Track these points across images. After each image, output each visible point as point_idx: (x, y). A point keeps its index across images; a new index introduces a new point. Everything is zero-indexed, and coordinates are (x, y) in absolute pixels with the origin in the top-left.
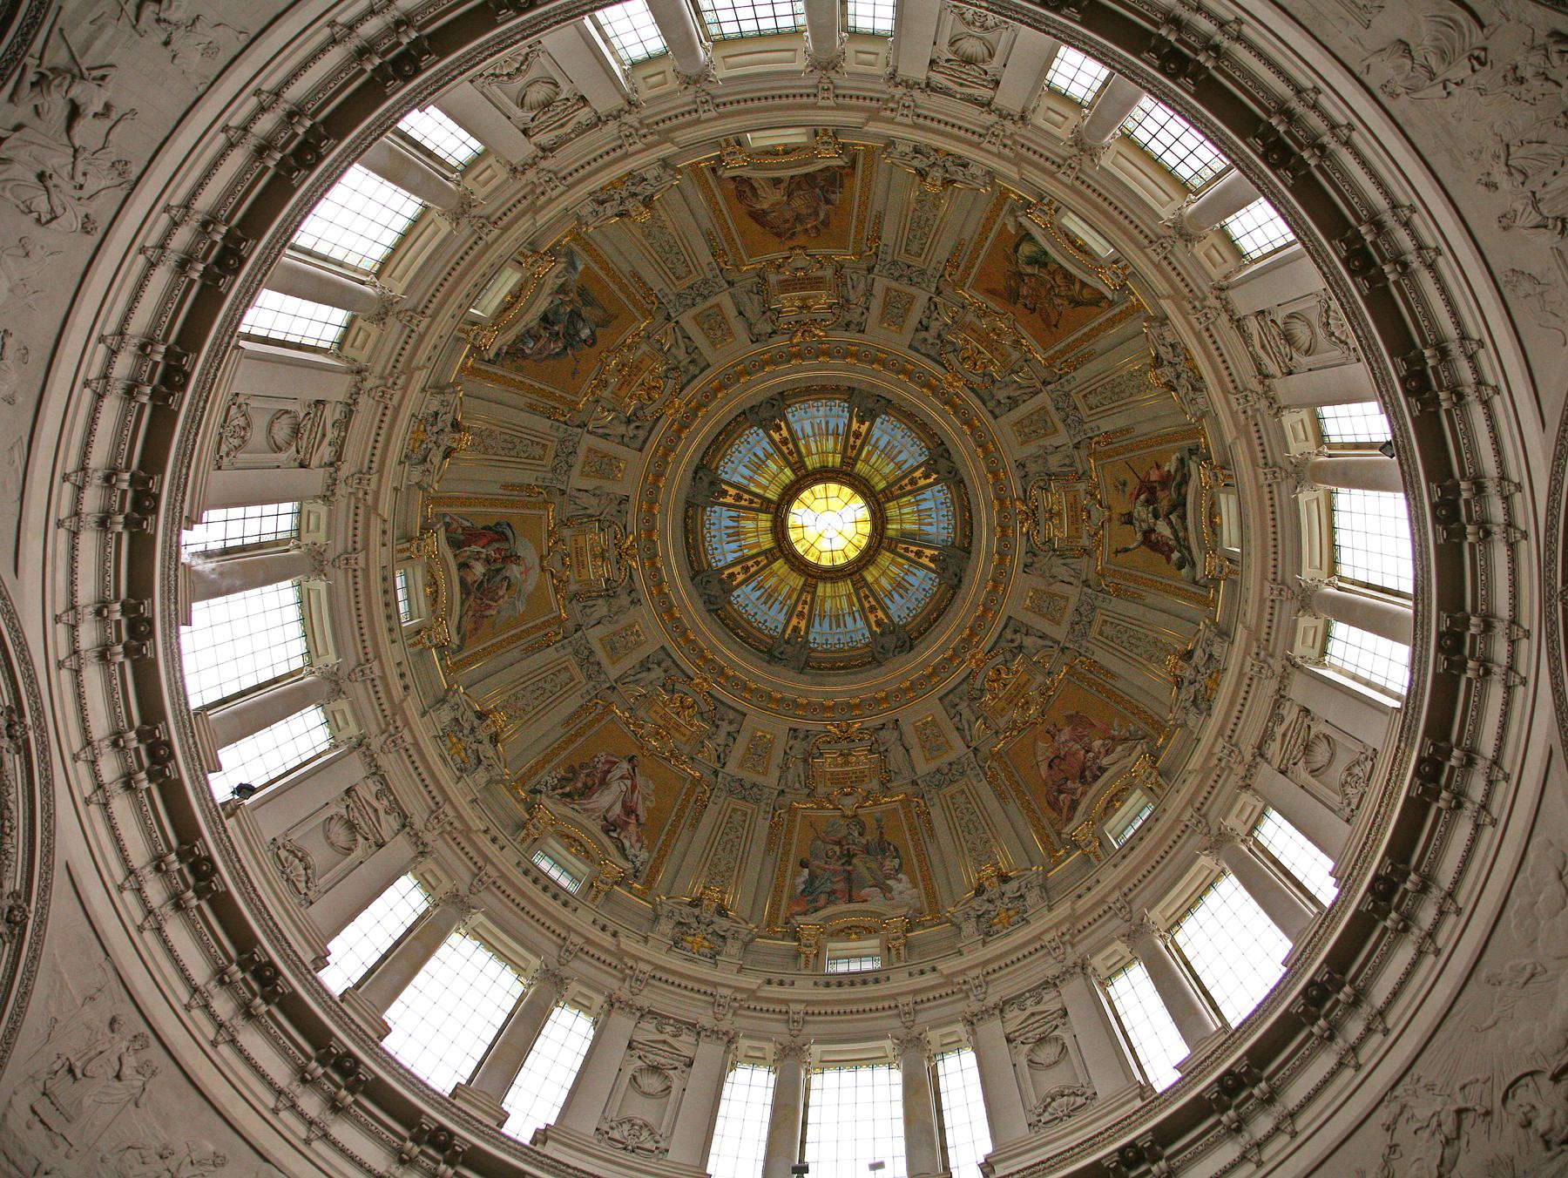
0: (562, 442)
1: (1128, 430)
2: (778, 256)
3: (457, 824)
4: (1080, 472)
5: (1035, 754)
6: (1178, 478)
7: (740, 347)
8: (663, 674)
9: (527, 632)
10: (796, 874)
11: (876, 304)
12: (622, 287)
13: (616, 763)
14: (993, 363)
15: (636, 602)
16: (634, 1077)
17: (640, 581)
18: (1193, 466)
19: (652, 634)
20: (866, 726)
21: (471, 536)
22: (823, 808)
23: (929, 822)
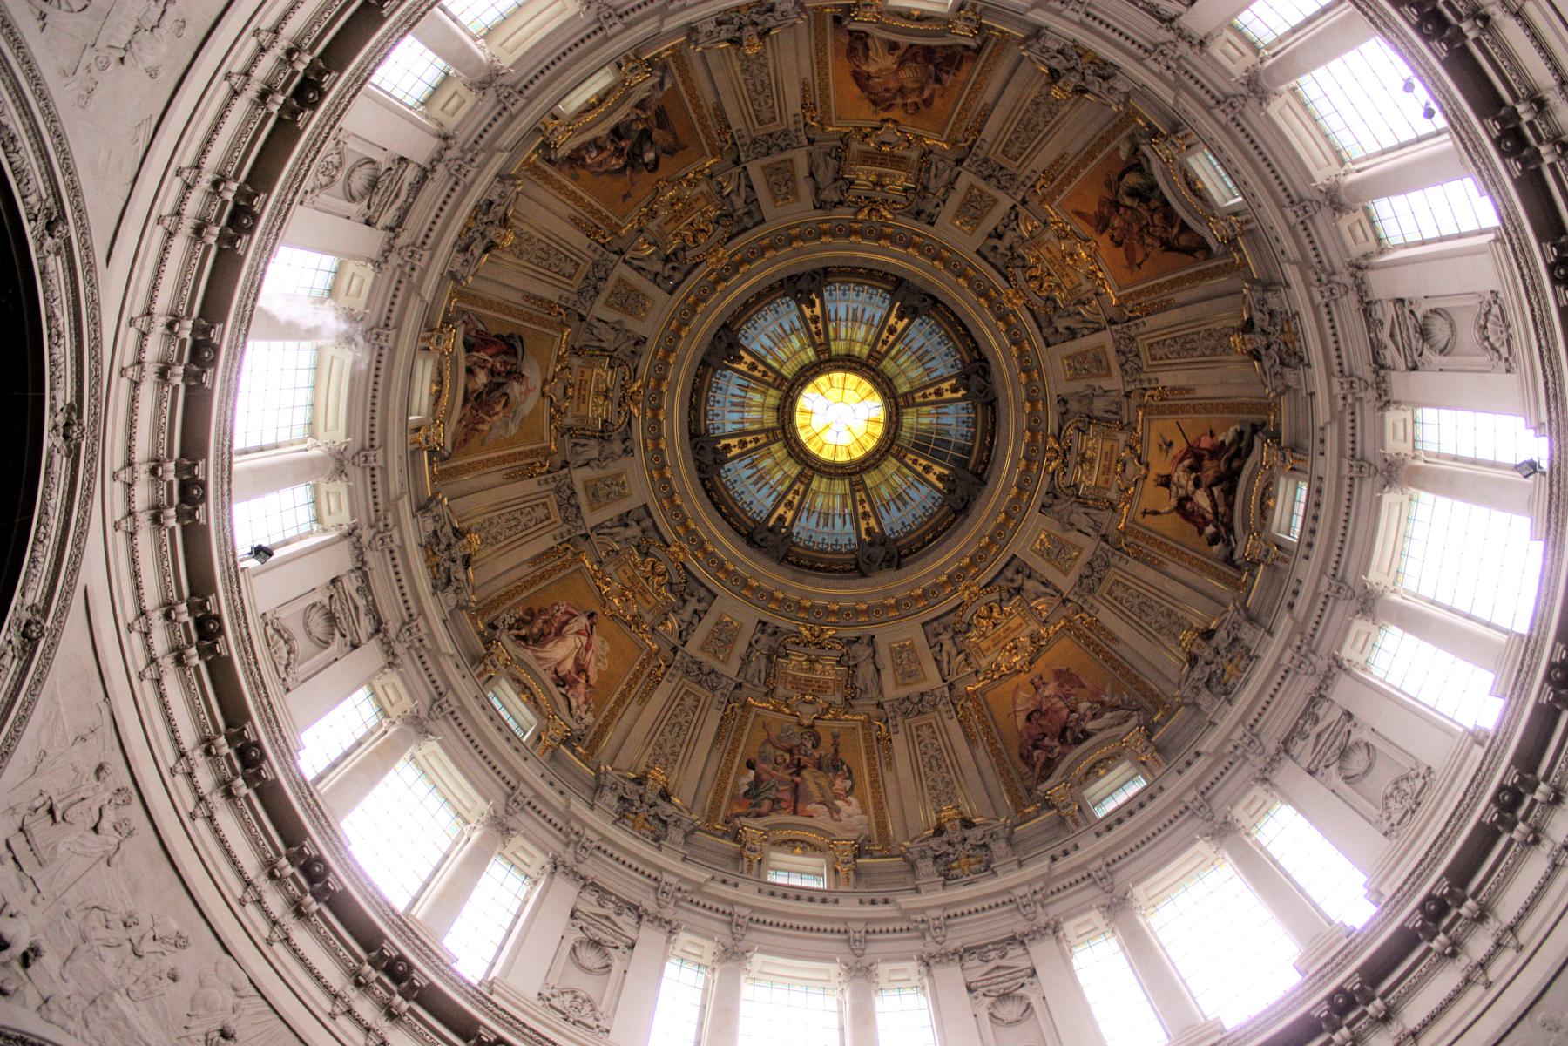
0: (596, 265)
4: (1126, 421)
5: (1014, 703)
6: (1232, 450)
7: (801, 210)
8: (640, 535)
9: (513, 457)
10: (739, 774)
11: (955, 200)
12: (701, 118)
13: (574, 616)
15: (628, 452)
18: (1257, 442)
19: (639, 490)
22: (779, 711)
23: (889, 749)
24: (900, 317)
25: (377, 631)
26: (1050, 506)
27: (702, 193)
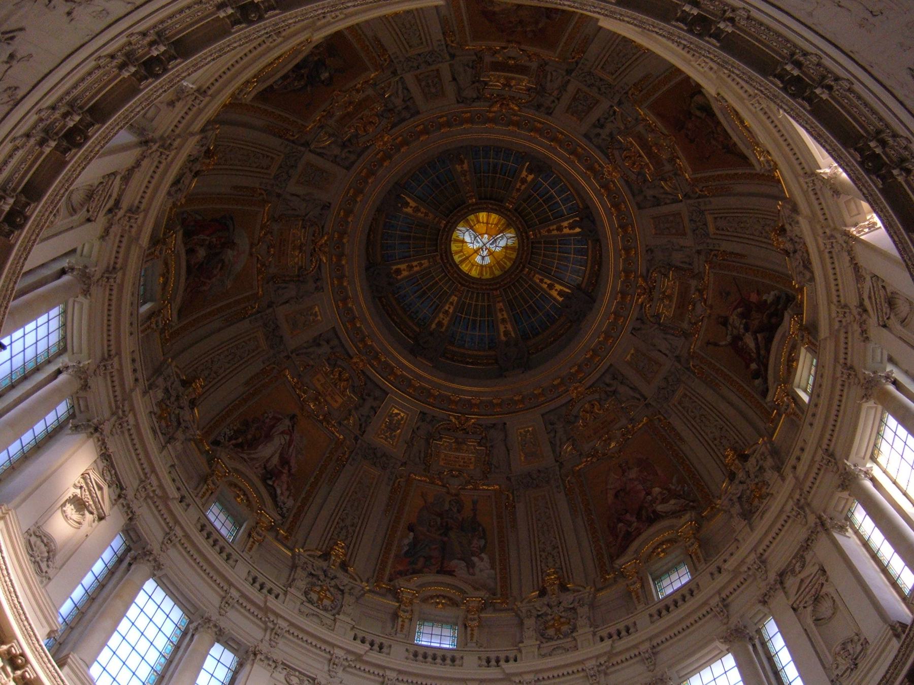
1: (742, 256)
4: (696, 271)
18: (787, 316)
22: (433, 483)
25: (119, 496)
26: (639, 329)
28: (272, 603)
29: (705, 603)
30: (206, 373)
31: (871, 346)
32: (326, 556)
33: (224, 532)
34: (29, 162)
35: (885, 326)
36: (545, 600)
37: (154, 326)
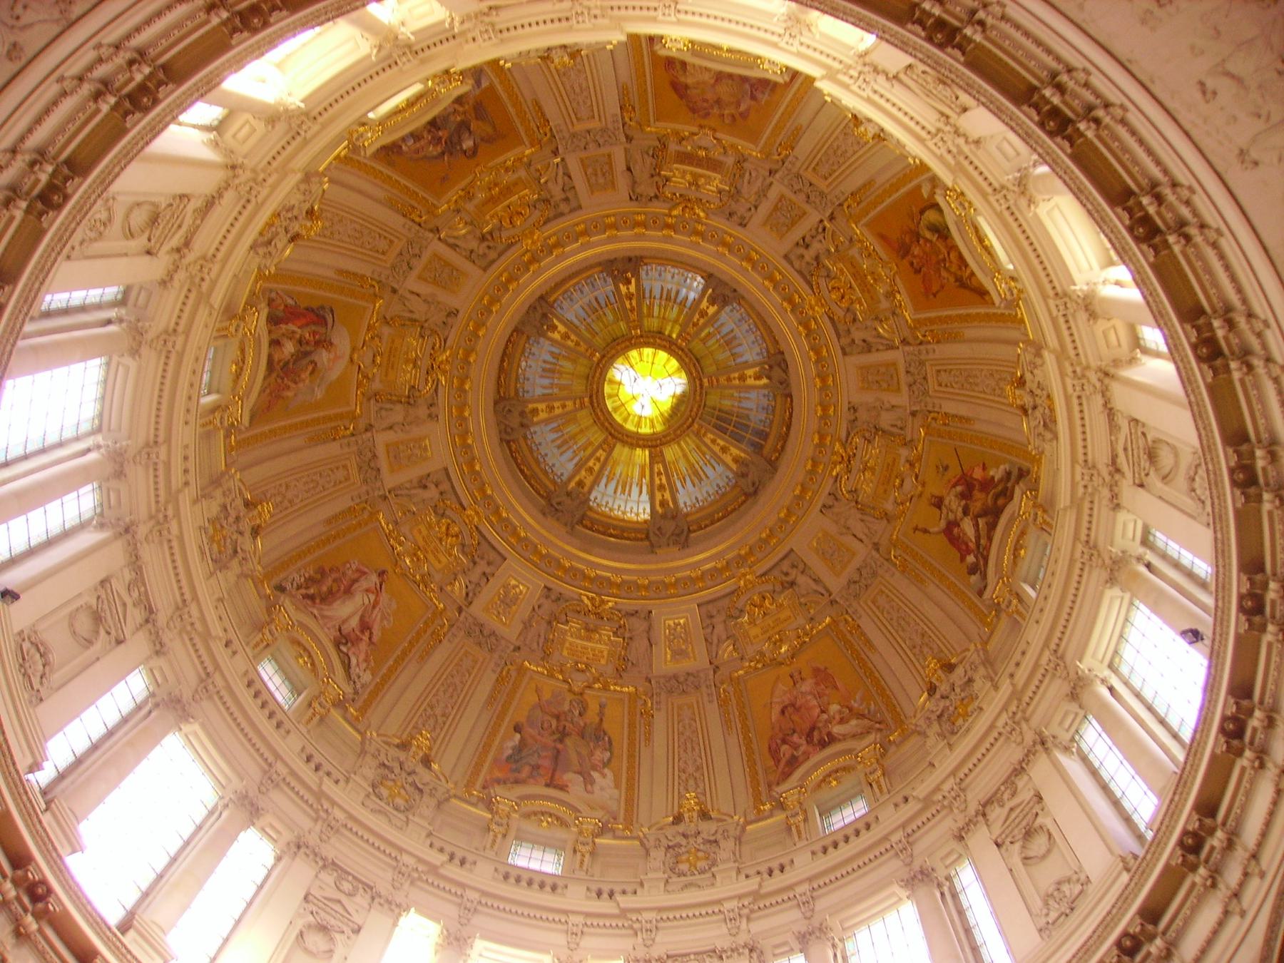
1: (968, 420)
2: (686, 130)
3: (198, 626)
4: (908, 438)
6: (1000, 488)
8: (437, 496)
9: (316, 421)
13: (365, 573)
14: (861, 304)
15: (433, 417)
16: (301, 934)
17: (442, 399)
18: (1017, 492)
20: (619, 607)
21: (292, 314)
22: (551, 676)
24: (712, 301)
25: (147, 621)
27: (520, 178)
28: (328, 787)
29: (886, 838)
30: (279, 499)
31: (1122, 516)
32: (404, 746)
33: (280, 698)
34: (78, 123)
35: (1141, 486)
36: (681, 828)
37: (217, 422)
